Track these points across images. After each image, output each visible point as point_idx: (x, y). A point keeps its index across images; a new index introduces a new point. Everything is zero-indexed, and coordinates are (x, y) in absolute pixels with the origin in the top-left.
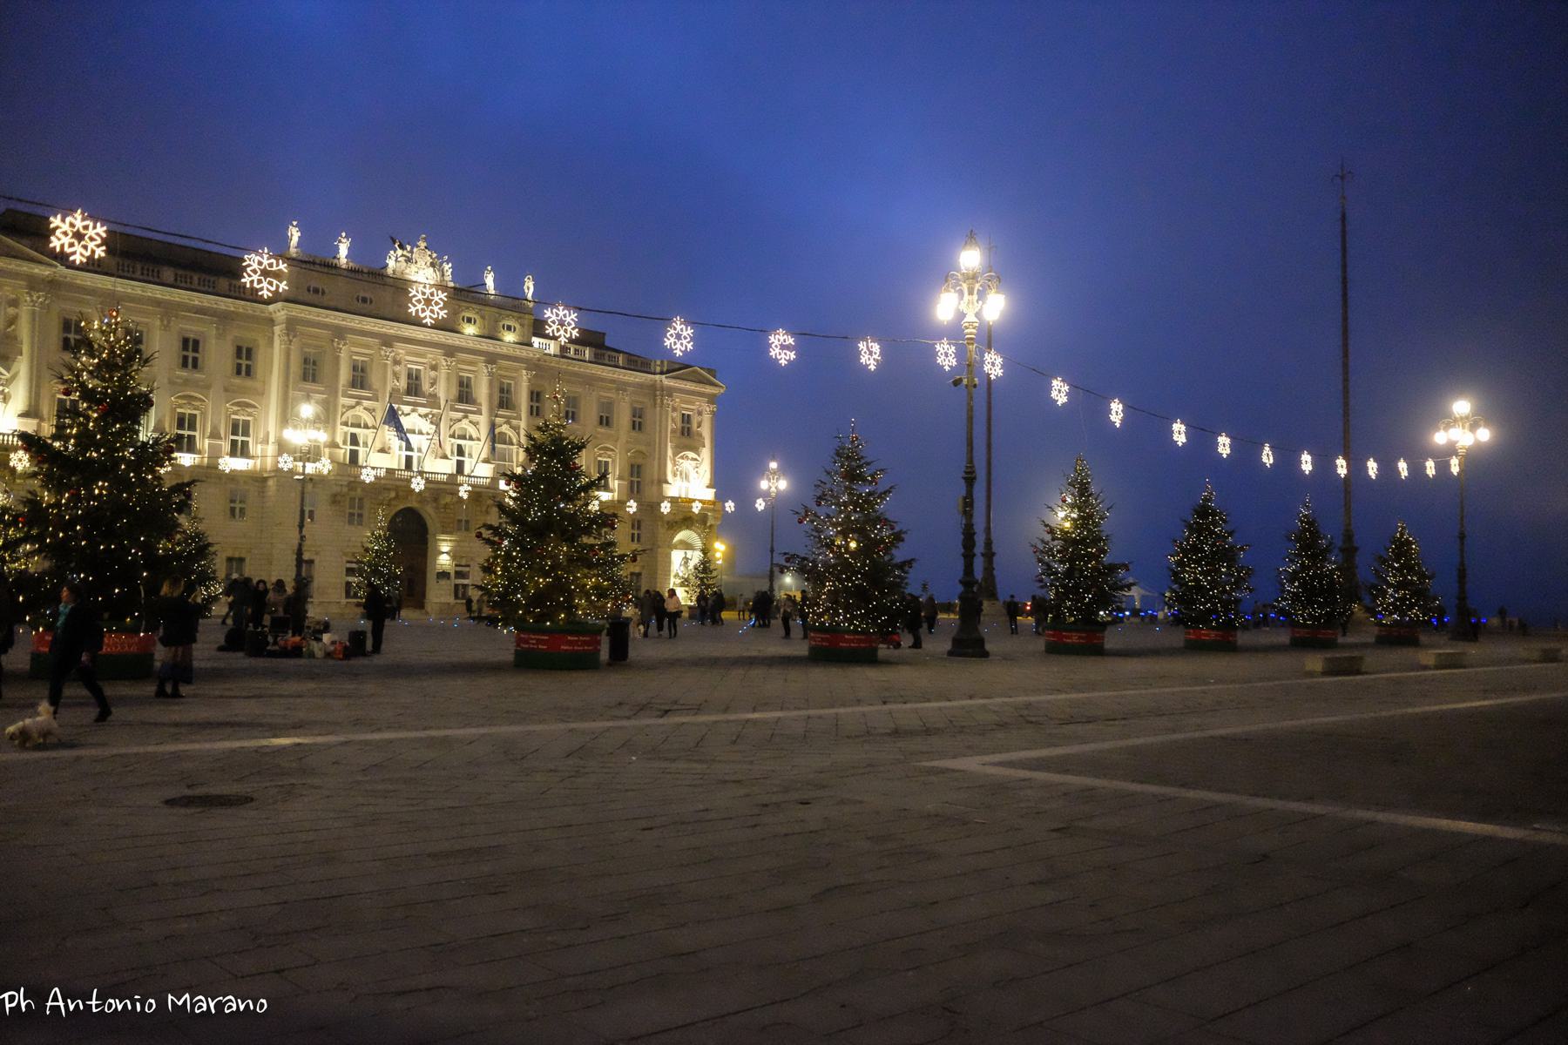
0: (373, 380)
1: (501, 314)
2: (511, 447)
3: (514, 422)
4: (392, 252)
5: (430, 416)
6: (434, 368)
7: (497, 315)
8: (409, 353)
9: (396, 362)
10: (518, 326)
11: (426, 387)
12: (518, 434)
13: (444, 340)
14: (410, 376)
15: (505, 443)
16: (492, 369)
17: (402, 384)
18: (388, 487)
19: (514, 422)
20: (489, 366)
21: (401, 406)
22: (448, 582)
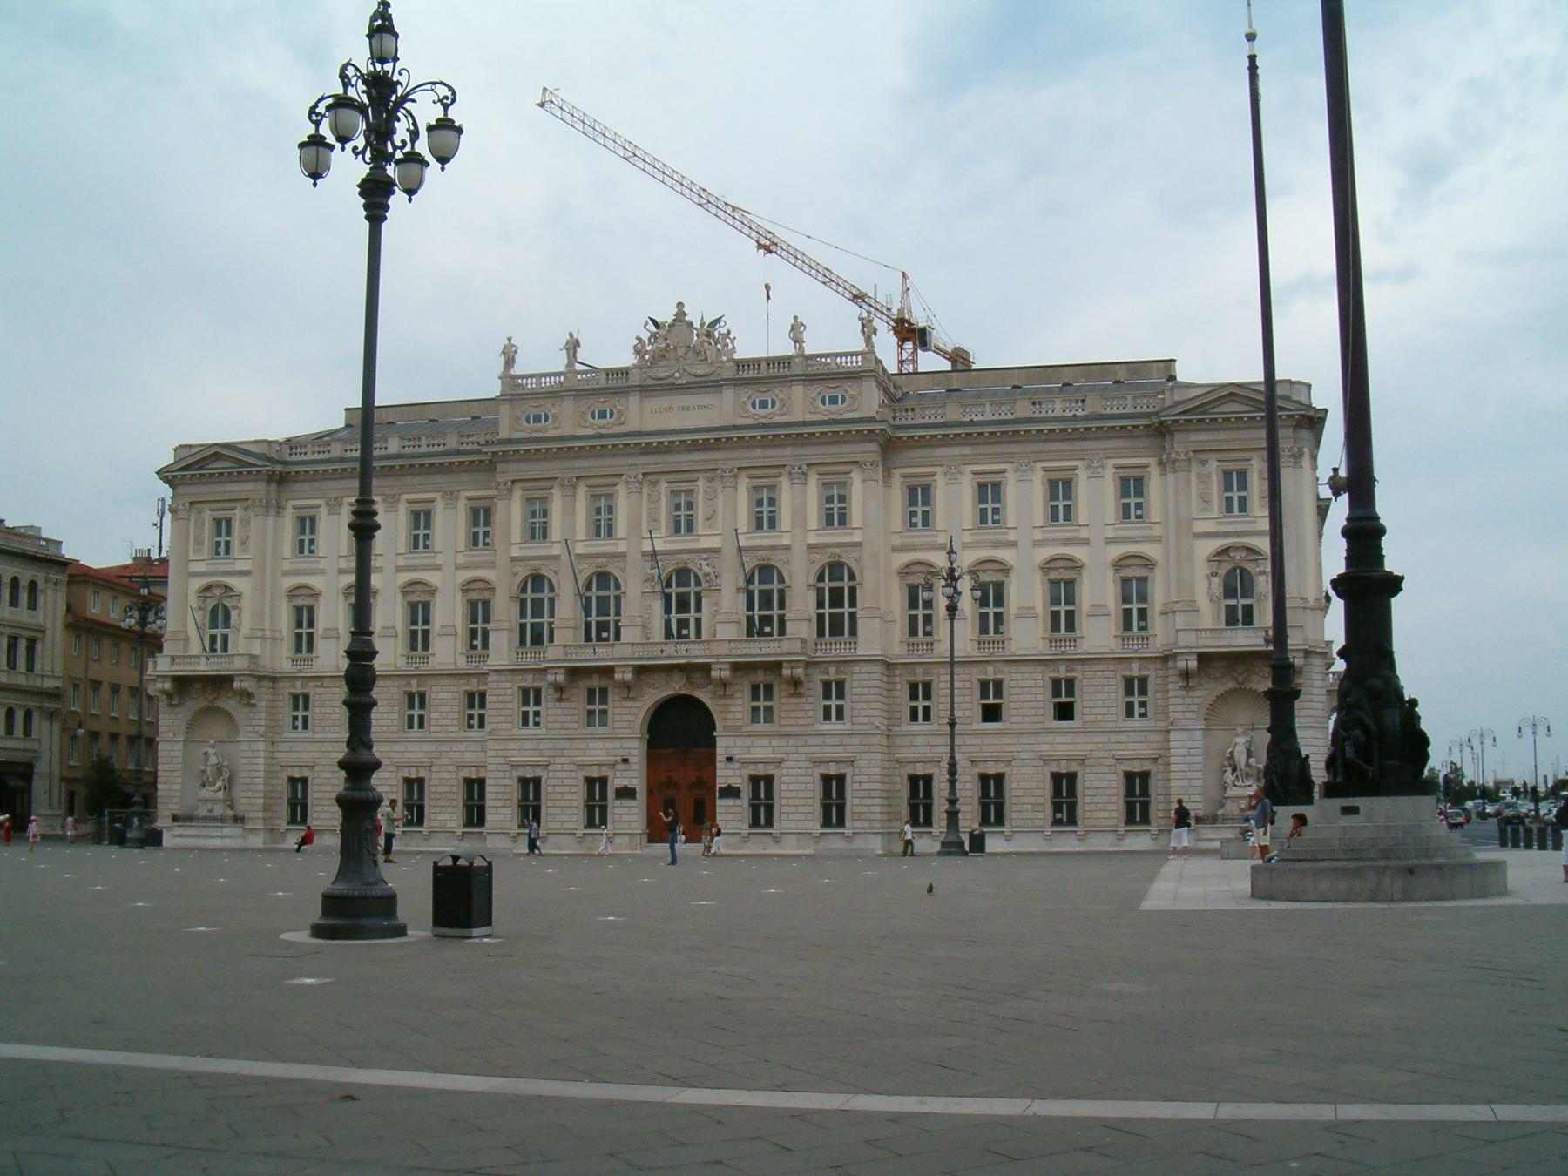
22: (738, 802)
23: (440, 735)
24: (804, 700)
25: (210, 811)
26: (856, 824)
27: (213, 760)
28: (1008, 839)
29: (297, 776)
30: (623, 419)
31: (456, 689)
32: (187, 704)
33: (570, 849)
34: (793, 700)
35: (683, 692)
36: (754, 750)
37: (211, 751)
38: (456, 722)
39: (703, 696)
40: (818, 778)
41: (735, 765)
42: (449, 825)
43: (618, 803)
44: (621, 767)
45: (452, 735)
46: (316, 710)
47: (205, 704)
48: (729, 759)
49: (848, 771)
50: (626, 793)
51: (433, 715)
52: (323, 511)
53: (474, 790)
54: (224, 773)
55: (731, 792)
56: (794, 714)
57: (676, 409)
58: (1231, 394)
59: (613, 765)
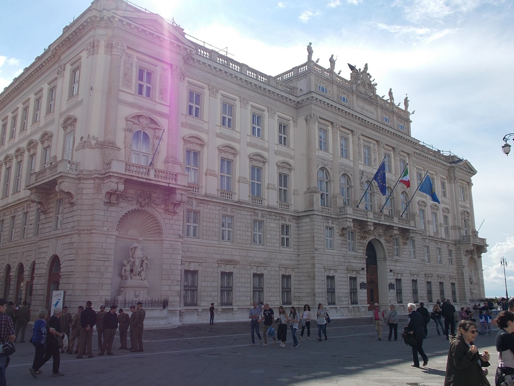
23: (270, 248)
25: (136, 296)
27: (139, 253)
31: (277, 222)
32: (121, 205)
33: (347, 316)
36: (397, 268)
37: (140, 247)
38: (278, 242)
39: (382, 240)
41: (392, 274)
44: (361, 272)
45: (278, 249)
46: (205, 224)
47: (135, 207)
48: (391, 271)
50: (362, 285)
52: (206, 92)
54: (144, 265)
57: (364, 110)
59: (358, 272)
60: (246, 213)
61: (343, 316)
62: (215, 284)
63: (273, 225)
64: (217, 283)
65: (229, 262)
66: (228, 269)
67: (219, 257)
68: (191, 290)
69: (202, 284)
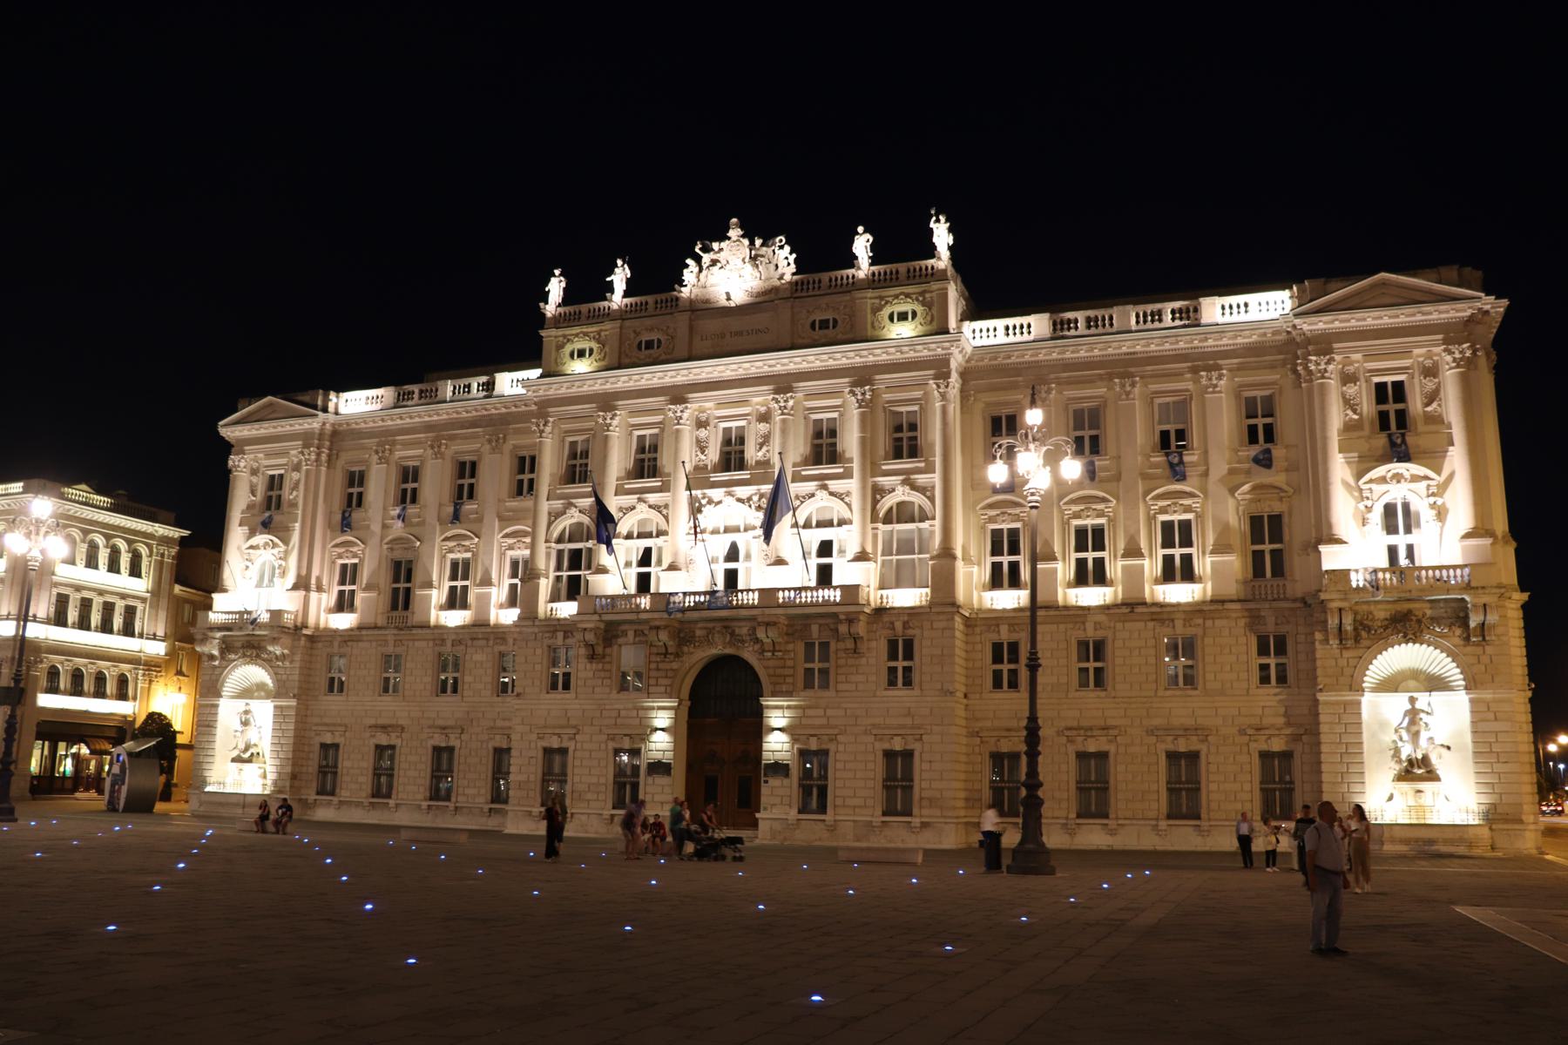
0: (664, 463)
1: (881, 298)
2: (925, 525)
3: (921, 479)
4: (689, 261)
5: (755, 498)
6: (765, 418)
7: (877, 301)
8: (720, 405)
9: (701, 424)
10: (919, 309)
11: (752, 453)
12: (932, 499)
13: (766, 369)
14: (727, 442)
15: (912, 520)
16: (864, 394)
17: (713, 455)
18: (657, 623)
19: (921, 479)
20: (858, 390)
21: (706, 491)
22: (786, 782)
24: (863, 661)
26: (925, 812)
28: (1112, 833)
29: (329, 742)
30: (671, 346)
33: (596, 833)
34: (851, 661)
35: (729, 651)
39: (749, 654)
40: (880, 755)
42: (477, 801)
43: (650, 780)
49: (917, 747)
51: (468, 679)
53: (442, 759)
55: (779, 769)
56: (853, 678)
58: (1384, 284)
60: (423, 644)
61: (586, 832)
62: (364, 764)
63: (478, 657)
64: (368, 764)
65: (384, 728)
66: (383, 740)
67: (372, 722)
68: (387, 775)
69: (346, 763)
